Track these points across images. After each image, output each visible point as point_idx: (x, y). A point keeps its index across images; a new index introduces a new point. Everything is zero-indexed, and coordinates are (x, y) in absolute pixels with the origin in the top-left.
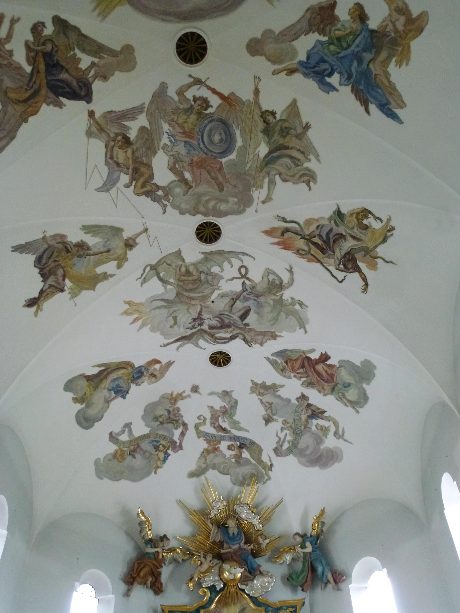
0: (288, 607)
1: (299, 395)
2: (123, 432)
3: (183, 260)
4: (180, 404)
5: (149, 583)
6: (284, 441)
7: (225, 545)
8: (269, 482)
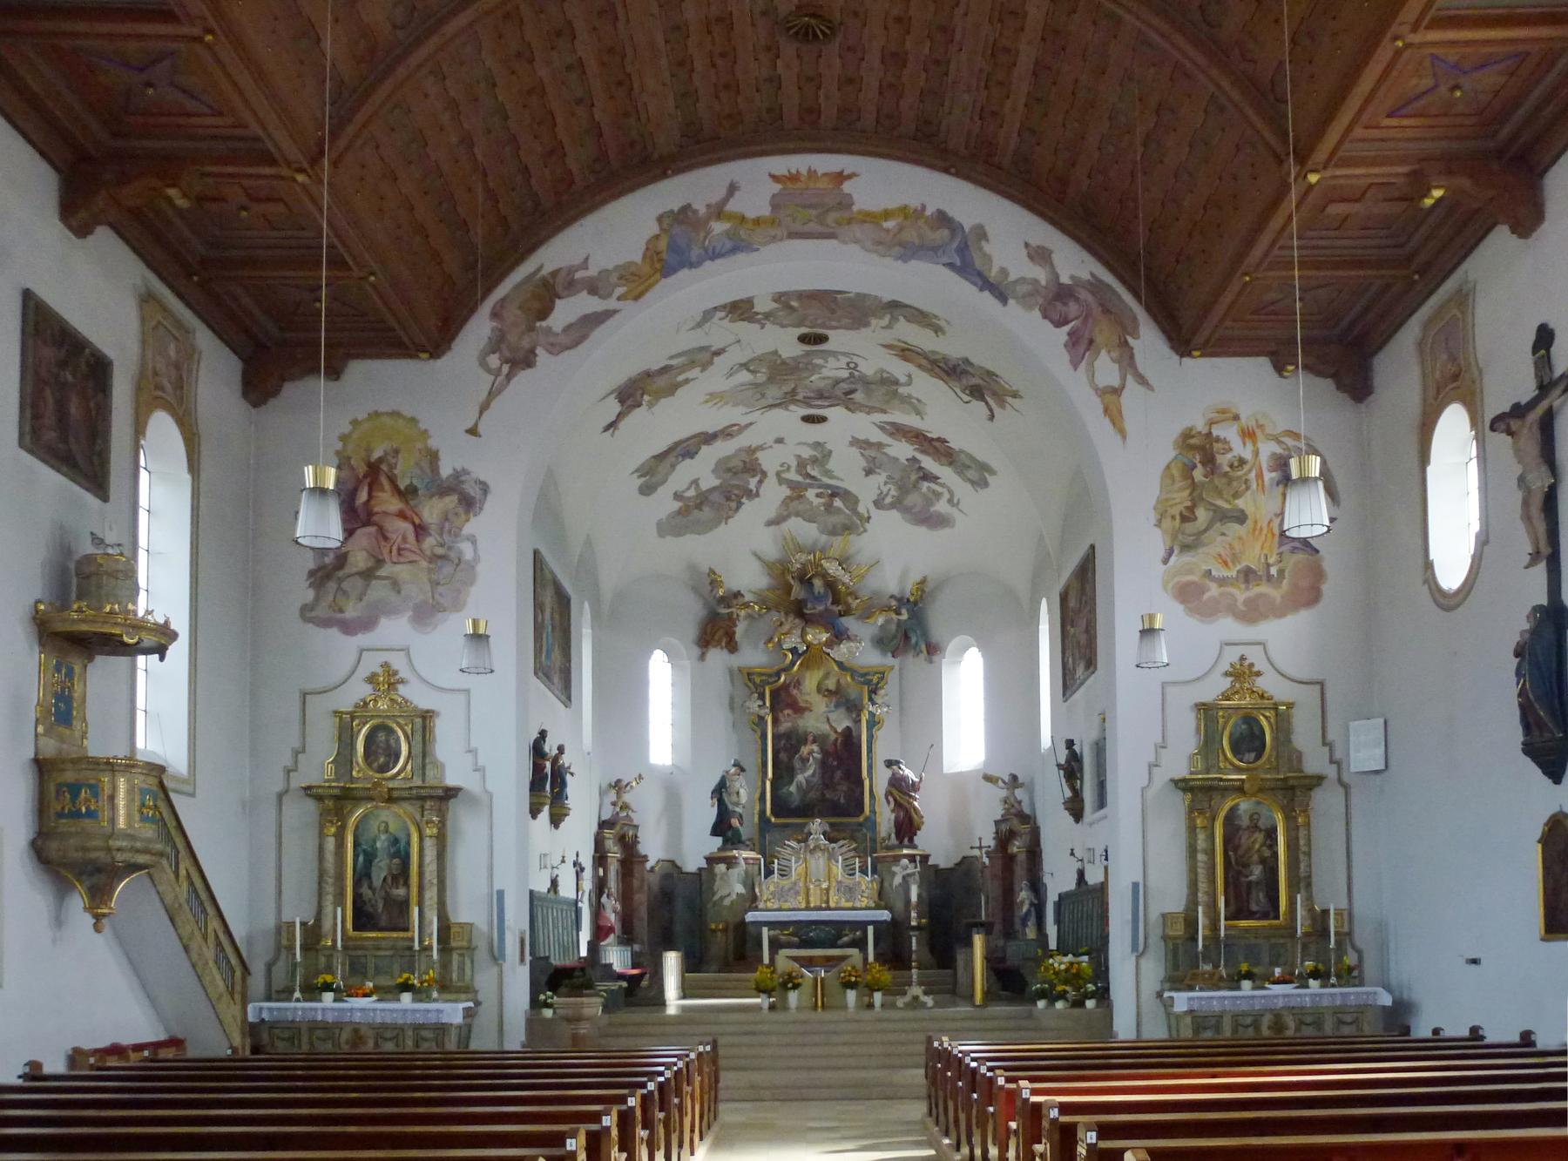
0: (877, 673)
1: (910, 457)
2: (688, 489)
3: (780, 356)
4: (759, 455)
5: (723, 644)
6: (887, 495)
7: (809, 605)
8: (865, 534)
